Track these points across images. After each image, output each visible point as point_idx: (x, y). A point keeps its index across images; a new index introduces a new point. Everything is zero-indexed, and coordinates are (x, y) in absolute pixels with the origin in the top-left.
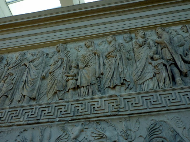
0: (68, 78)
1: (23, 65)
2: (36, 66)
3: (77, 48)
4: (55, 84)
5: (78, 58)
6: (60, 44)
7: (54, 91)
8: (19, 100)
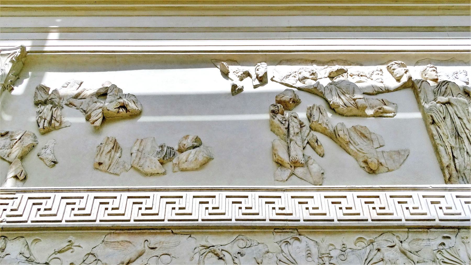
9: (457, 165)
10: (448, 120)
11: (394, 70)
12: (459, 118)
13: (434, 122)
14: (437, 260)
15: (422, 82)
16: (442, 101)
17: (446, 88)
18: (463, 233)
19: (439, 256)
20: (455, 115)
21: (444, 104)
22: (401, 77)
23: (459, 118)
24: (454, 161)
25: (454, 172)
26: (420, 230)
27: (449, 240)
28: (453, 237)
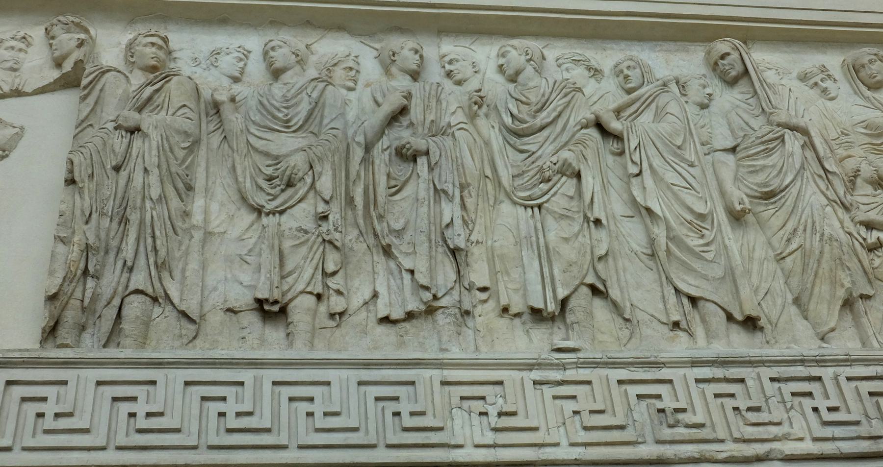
0: (878, 238)
1: (586, 127)
2: (679, 148)
3: (817, 79)
4: (827, 256)
5: (842, 133)
6: (737, 42)
7: (841, 293)
8: (676, 317)
9: (89, 294)
10: (124, 174)
11: (53, 38)
15: (104, 73)
16: (125, 125)
17: (157, 91)
20: (140, 160)
22: (64, 57)
24: (85, 284)
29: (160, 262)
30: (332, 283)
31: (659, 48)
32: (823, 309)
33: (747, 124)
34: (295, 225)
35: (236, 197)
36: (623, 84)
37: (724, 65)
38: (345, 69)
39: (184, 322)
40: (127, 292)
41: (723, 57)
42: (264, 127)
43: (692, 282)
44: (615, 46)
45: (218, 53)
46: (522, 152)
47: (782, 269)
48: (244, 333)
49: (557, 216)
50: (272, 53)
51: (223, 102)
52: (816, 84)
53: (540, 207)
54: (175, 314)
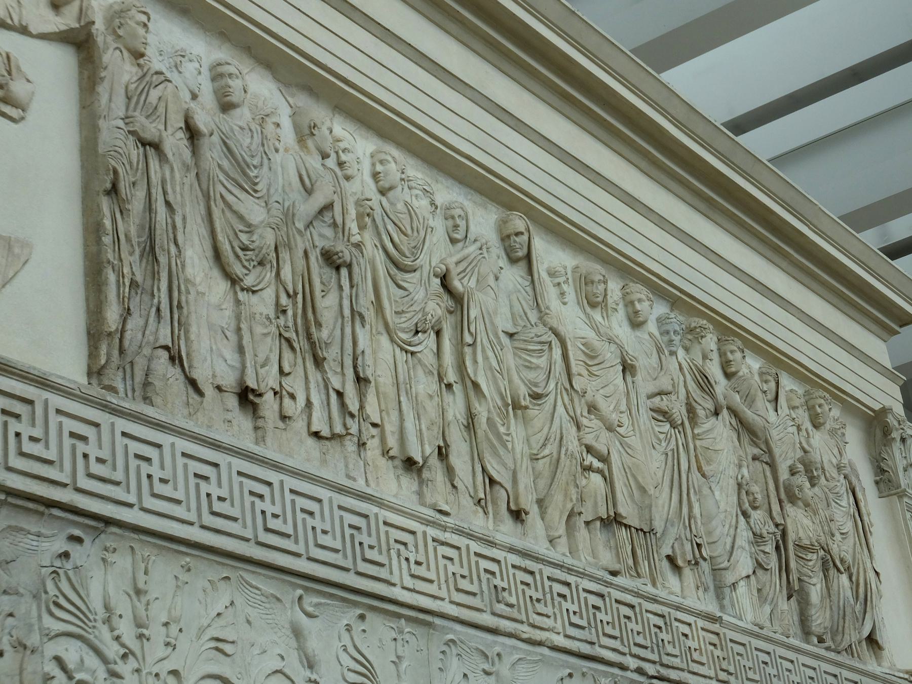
9: (128, 335)
12: (168, 204)
13: (113, 190)
14: (43, 595)
16: (142, 135)
18: (110, 538)
19: (50, 586)
21: (144, 143)
23: (168, 204)
25: (116, 353)
26: (31, 505)
27: (78, 547)
28: (87, 540)
29: (183, 320)
30: (286, 382)
31: (469, 197)
32: (556, 515)
33: (526, 314)
34: (265, 312)
35: (210, 253)
36: (450, 230)
37: (515, 242)
38: (274, 123)
39: (191, 391)
40: (158, 345)
41: (517, 234)
42: (233, 179)
43: (495, 466)
44: (444, 181)
45: (183, 56)
46: (400, 287)
47: (533, 468)
48: (229, 416)
49: (427, 371)
50: (230, 82)
51: (205, 135)
52: (559, 284)
53: (413, 353)
54: (182, 378)
